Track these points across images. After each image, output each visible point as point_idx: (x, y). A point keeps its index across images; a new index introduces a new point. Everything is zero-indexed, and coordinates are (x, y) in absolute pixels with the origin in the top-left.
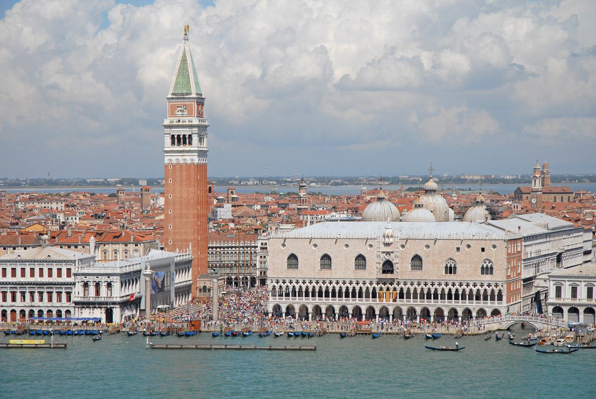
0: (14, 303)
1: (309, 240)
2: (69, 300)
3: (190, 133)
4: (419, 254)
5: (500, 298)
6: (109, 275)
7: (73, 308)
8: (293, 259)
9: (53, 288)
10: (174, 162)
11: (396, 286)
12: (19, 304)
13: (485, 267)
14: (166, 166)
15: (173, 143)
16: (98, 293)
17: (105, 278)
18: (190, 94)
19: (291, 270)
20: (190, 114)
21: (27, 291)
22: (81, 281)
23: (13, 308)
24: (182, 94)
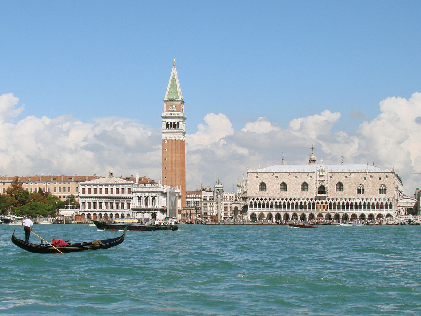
0: (95, 210)
1: (273, 173)
2: (129, 208)
3: (178, 122)
4: (341, 182)
5: (391, 207)
6: (154, 192)
7: (132, 213)
8: (263, 186)
9: (119, 200)
10: (168, 138)
11: (327, 201)
12: (98, 210)
13: (381, 189)
14: (163, 141)
15: (167, 127)
16: (147, 204)
17: (151, 195)
18: (178, 98)
19: (261, 192)
20: (178, 110)
21: (103, 202)
22: (137, 196)
23: (95, 212)
24: (173, 98)
